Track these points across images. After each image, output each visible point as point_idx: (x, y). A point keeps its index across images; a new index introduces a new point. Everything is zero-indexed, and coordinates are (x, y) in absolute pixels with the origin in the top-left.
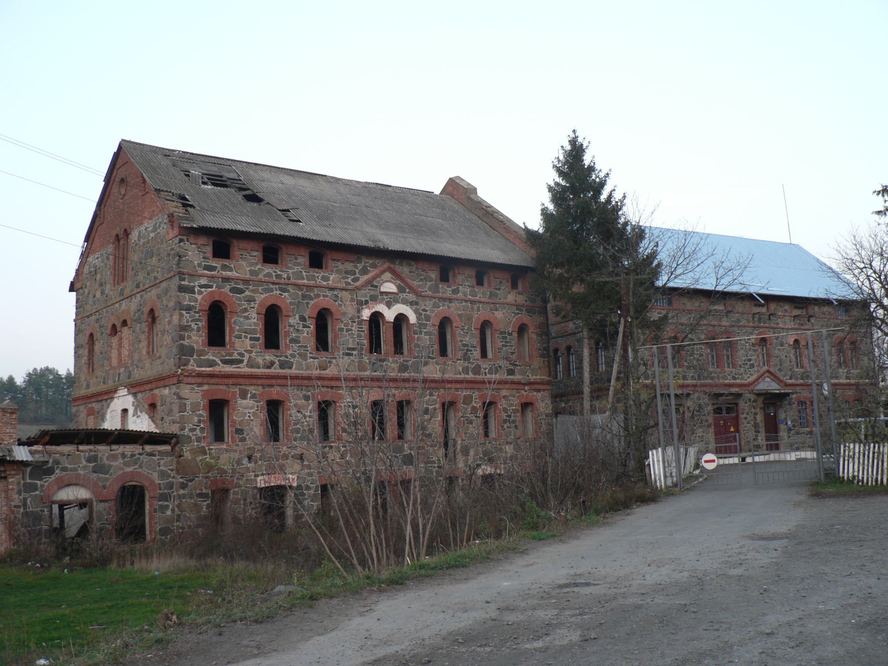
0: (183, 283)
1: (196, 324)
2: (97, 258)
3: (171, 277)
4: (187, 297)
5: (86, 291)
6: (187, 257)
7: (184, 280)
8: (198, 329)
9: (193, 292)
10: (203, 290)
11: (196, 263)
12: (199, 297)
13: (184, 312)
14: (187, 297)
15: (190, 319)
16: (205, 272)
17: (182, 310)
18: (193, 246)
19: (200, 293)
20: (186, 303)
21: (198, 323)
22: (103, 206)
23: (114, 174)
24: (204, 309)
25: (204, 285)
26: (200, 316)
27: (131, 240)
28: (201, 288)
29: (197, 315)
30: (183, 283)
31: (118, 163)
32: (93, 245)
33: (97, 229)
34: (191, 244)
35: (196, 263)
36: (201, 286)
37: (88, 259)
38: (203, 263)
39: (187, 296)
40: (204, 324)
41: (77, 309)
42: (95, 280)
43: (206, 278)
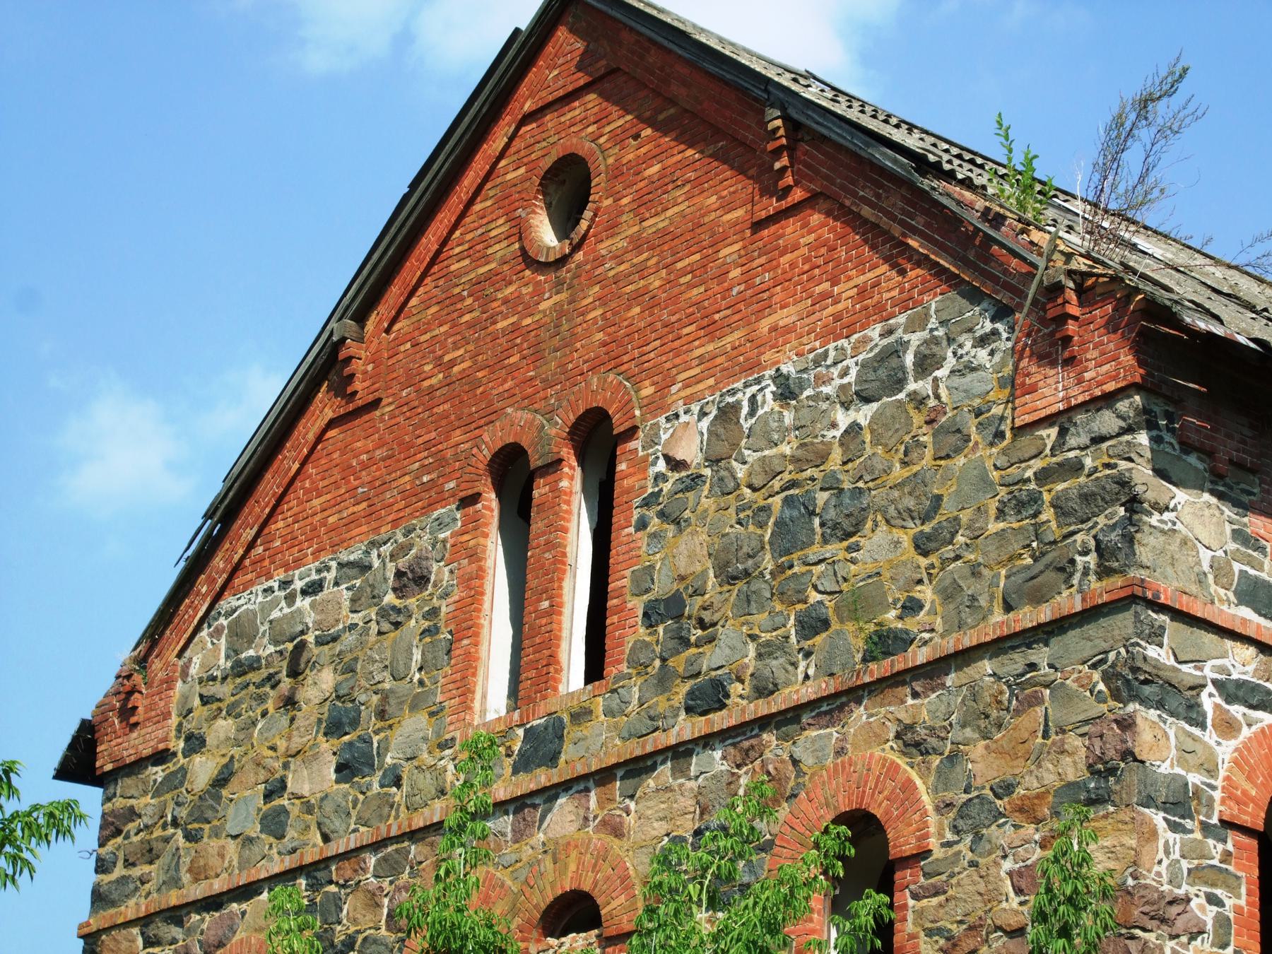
0: (1152, 651)
1: (1213, 900)
2: (313, 589)
3: (1060, 626)
4: (1171, 733)
5: (203, 769)
6: (1167, 516)
7: (1156, 636)
8: (1223, 922)
9: (1193, 714)
10: (1237, 710)
11: (1205, 556)
12: (1225, 751)
13: (1158, 818)
14: (1171, 733)
15: (1185, 865)
16: (1246, 612)
17: (1149, 802)
18: (1192, 459)
19: (1228, 727)
20: (1165, 769)
21: (1219, 892)
22: (383, 311)
23: (497, 141)
24: (1246, 820)
25: (1240, 684)
26: (1227, 856)
27: (644, 463)
28: (1230, 699)
29: (1215, 849)
30: (1152, 651)
31: (523, 89)
32: (279, 525)
33: (319, 438)
34: (1187, 447)
35: (1205, 556)
36: (1232, 691)
37: (224, 605)
38: (1237, 567)
39: (1174, 728)
40: (1242, 902)
41: (102, 866)
42: (290, 702)
43: (1252, 651)
